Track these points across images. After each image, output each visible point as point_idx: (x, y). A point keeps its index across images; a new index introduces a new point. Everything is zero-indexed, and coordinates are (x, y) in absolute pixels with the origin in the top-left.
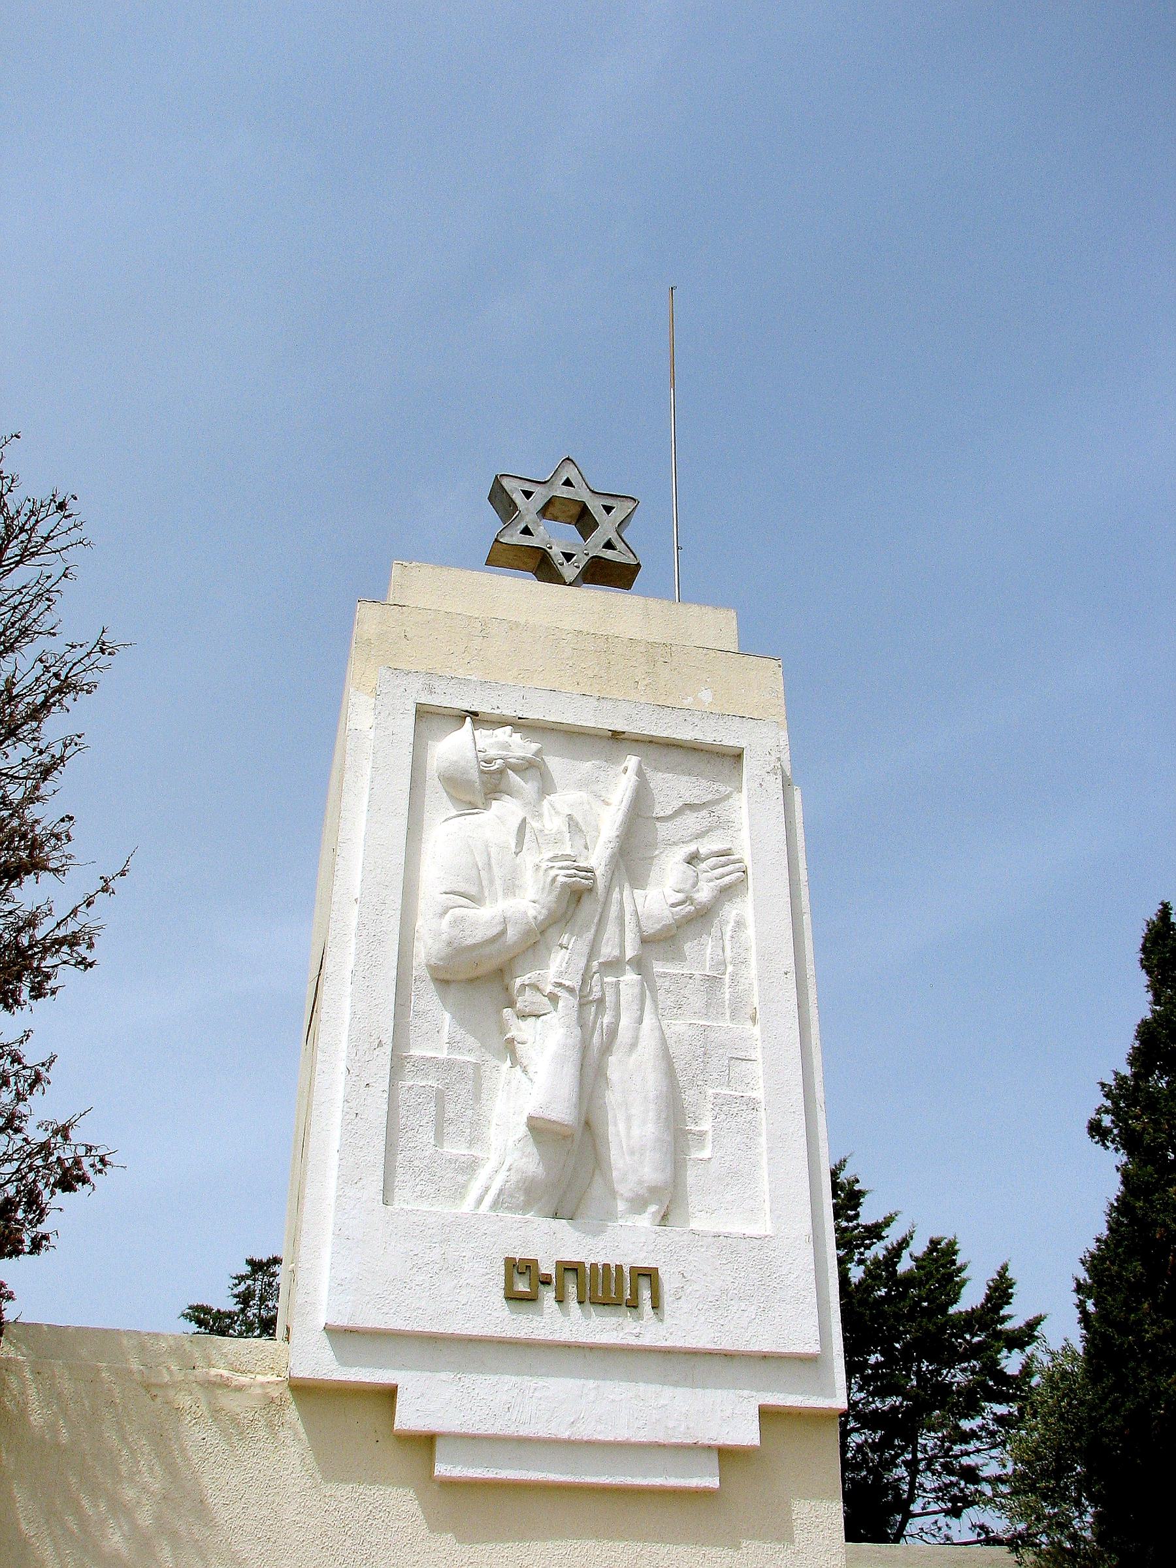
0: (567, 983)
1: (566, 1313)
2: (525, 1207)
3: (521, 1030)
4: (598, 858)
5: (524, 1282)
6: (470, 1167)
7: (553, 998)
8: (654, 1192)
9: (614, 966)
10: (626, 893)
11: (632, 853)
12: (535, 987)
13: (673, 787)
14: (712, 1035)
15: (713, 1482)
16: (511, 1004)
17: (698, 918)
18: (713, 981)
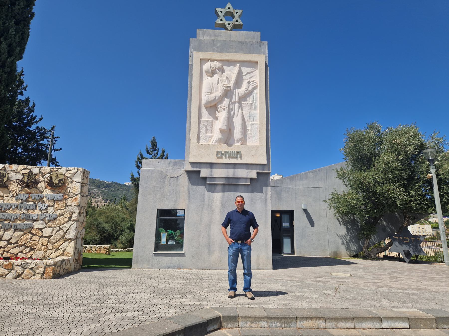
3: (218, 114)
4: (231, 85)
6: (211, 137)
7: (224, 109)
8: (240, 140)
9: (235, 103)
12: (221, 107)
13: (245, 70)
14: (251, 113)
16: (217, 110)
17: (249, 93)
18: (251, 104)
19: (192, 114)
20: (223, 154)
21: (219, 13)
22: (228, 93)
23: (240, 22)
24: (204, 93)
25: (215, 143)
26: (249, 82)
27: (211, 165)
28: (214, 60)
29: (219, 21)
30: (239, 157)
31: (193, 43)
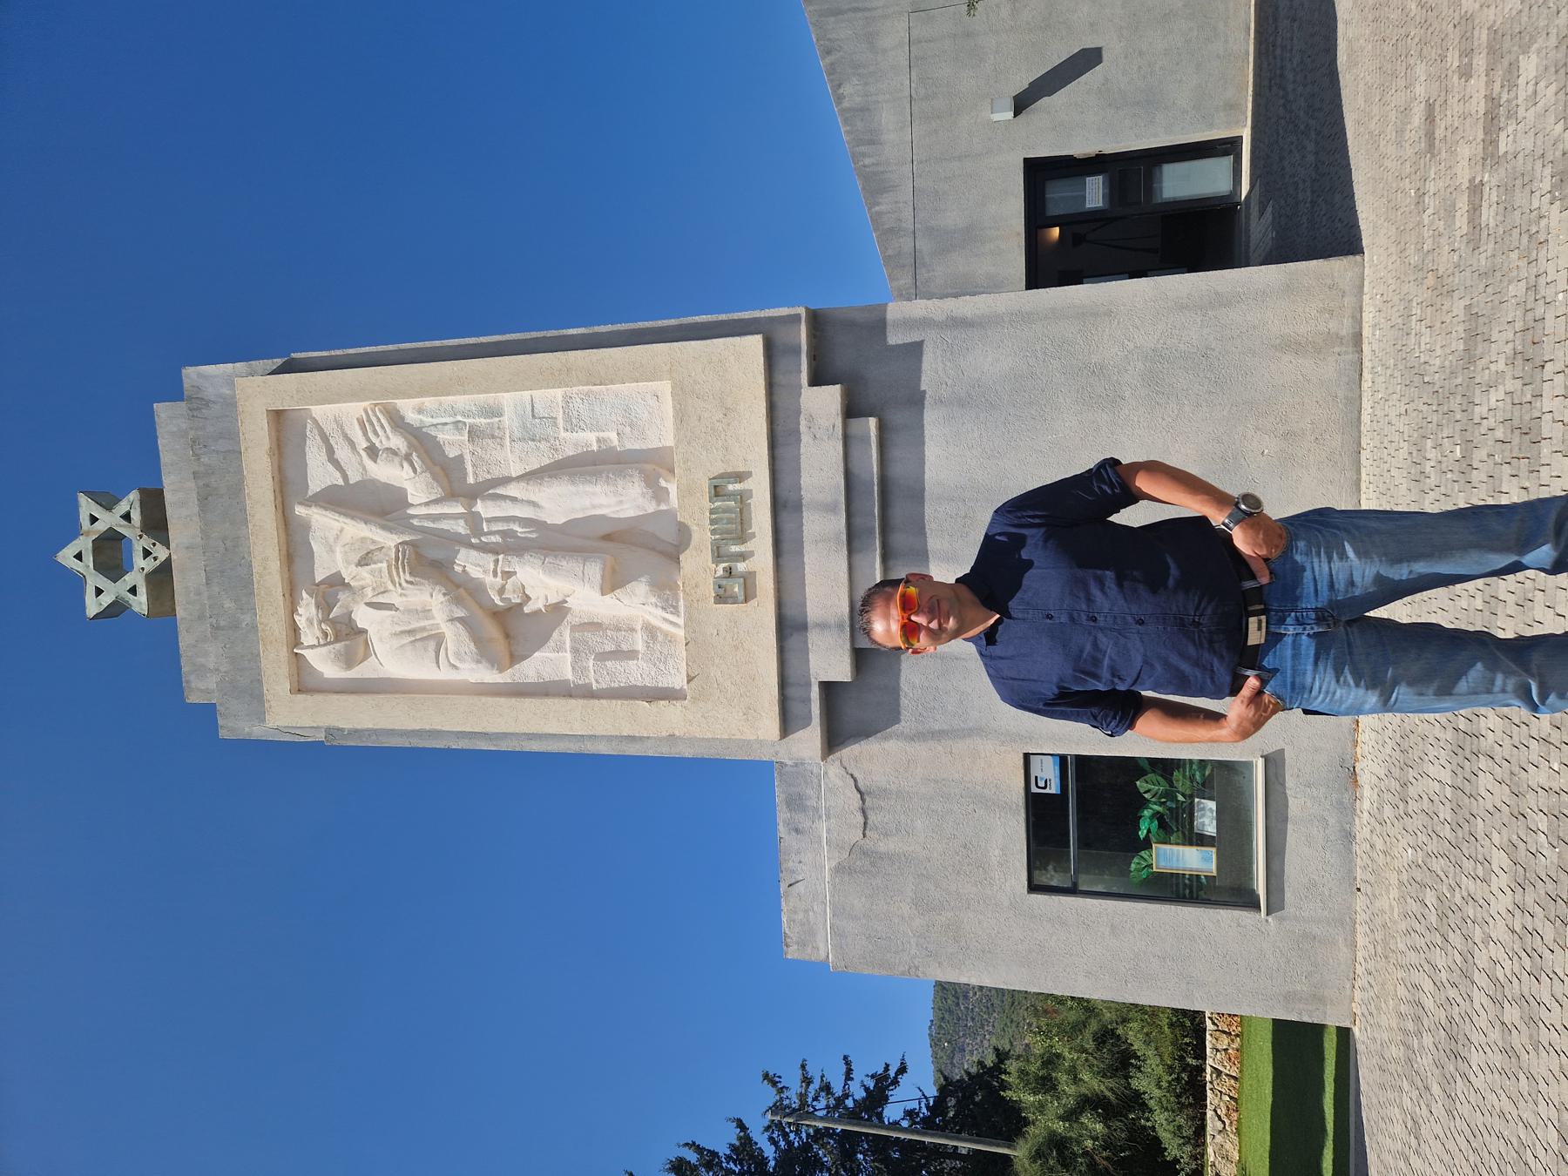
0: (492, 567)
1: (751, 554)
2: (673, 588)
4: (390, 540)
5: (732, 588)
6: (651, 631)
7: (508, 575)
8: (651, 482)
9: (474, 520)
10: (411, 511)
11: (381, 506)
12: (501, 591)
13: (320, 475)
14: (517, 434)
15: (872, 422)
16: (520, 605)
17: (423, 445)
18: (474, 434)
19: (551, 731)
20: (729, 572)
21: (106, 600)
22: (428, 560)
23: (131, 502)
24: (444, 674)
25: (676, 612)
26: (373, 452)
27: (789, 628)
28: (295, 629)
29: (140, 603)
30: (738, 487)
31: (235, 725)
